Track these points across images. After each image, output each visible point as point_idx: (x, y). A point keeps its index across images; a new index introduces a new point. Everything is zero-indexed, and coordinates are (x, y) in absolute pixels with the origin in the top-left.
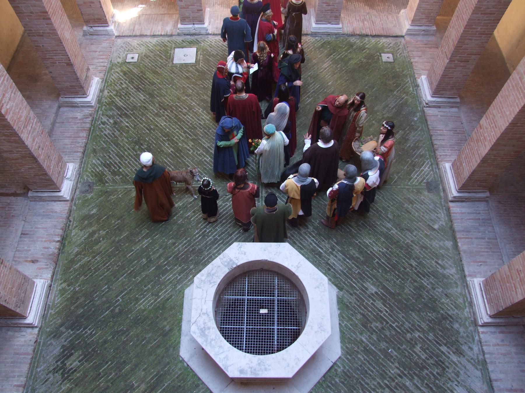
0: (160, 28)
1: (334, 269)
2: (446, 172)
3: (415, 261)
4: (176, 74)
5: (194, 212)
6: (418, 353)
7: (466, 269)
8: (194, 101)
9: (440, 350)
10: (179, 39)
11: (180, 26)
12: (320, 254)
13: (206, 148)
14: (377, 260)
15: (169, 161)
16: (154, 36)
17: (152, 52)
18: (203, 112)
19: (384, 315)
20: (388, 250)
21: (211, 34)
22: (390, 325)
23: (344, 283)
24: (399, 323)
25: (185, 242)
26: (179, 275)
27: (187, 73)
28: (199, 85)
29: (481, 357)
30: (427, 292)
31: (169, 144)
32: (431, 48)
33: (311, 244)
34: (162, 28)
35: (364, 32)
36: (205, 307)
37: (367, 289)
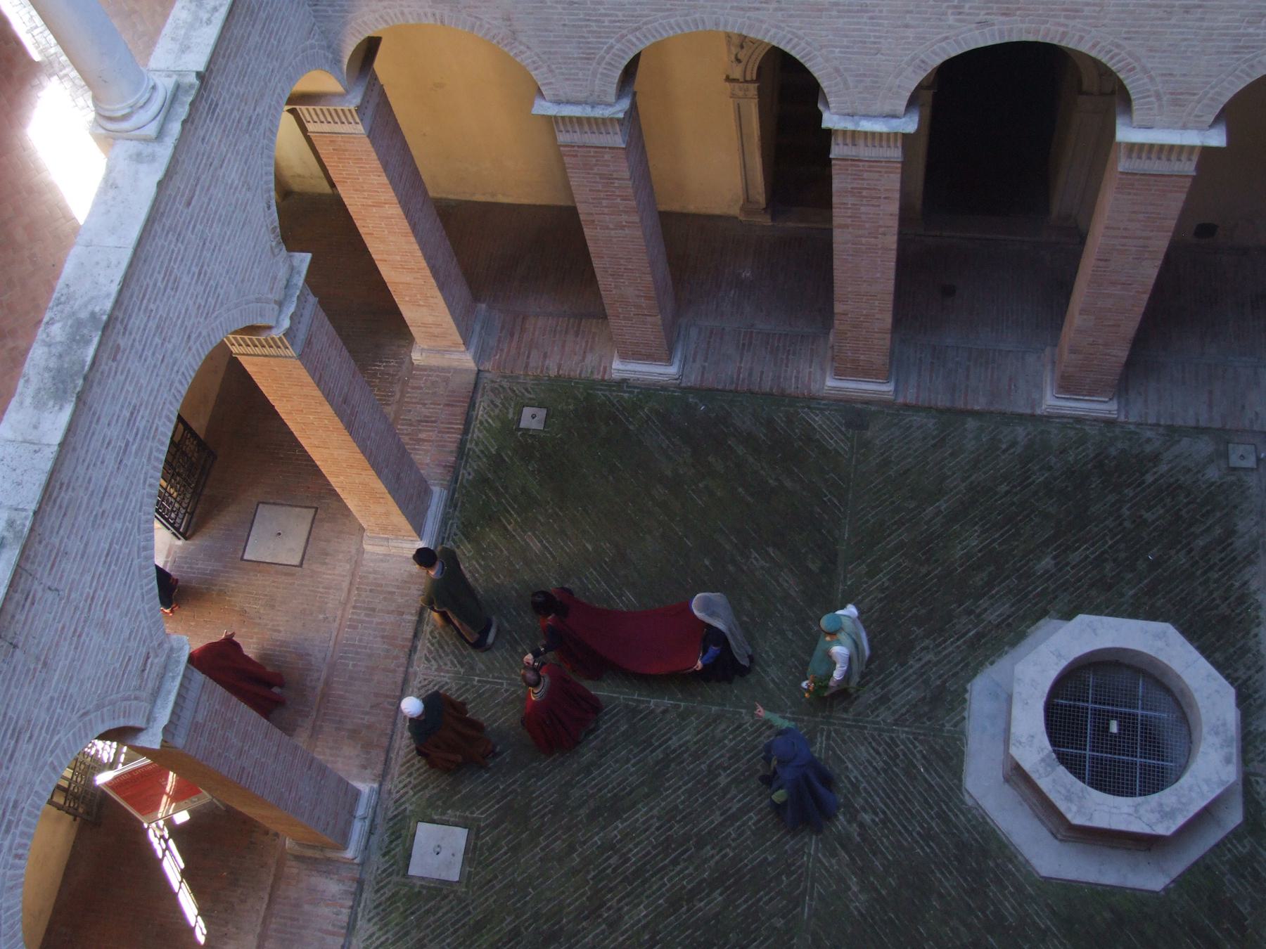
0: (325, 911)
1: (1009, 616)
2: (840, 389)
3: (1001, 483)
4: (496, 877)
5: (874, 855)
6: (1154, 517)
7: (1021, 411)
8: (591, 838)
9: (1151, 485)
10: (378, 862)
11: (349, 854)
12: (979, 636)
13: (725, 820)
14: (995, 545)
15: (746, 901)
16: (351, 928)
17: (407, 934)
18: (626, 820)
19: (1093, 553)
20: (976, 523)
21: (381, 785)
22: (1110, 547)
23: (1036, 604)
24: (1105, 535)
25: (938, 875)
26: (1007, 888)
27: (499, 850)
28: (543, 825)
29: (1161, 430)
30: (1055, 479)
31: (701, 900)
32: (523, 330)
33: (958, 647)
34: (327, 905)
35: (453, 447)
36: (1125, 809)
37: (1047, 571)
